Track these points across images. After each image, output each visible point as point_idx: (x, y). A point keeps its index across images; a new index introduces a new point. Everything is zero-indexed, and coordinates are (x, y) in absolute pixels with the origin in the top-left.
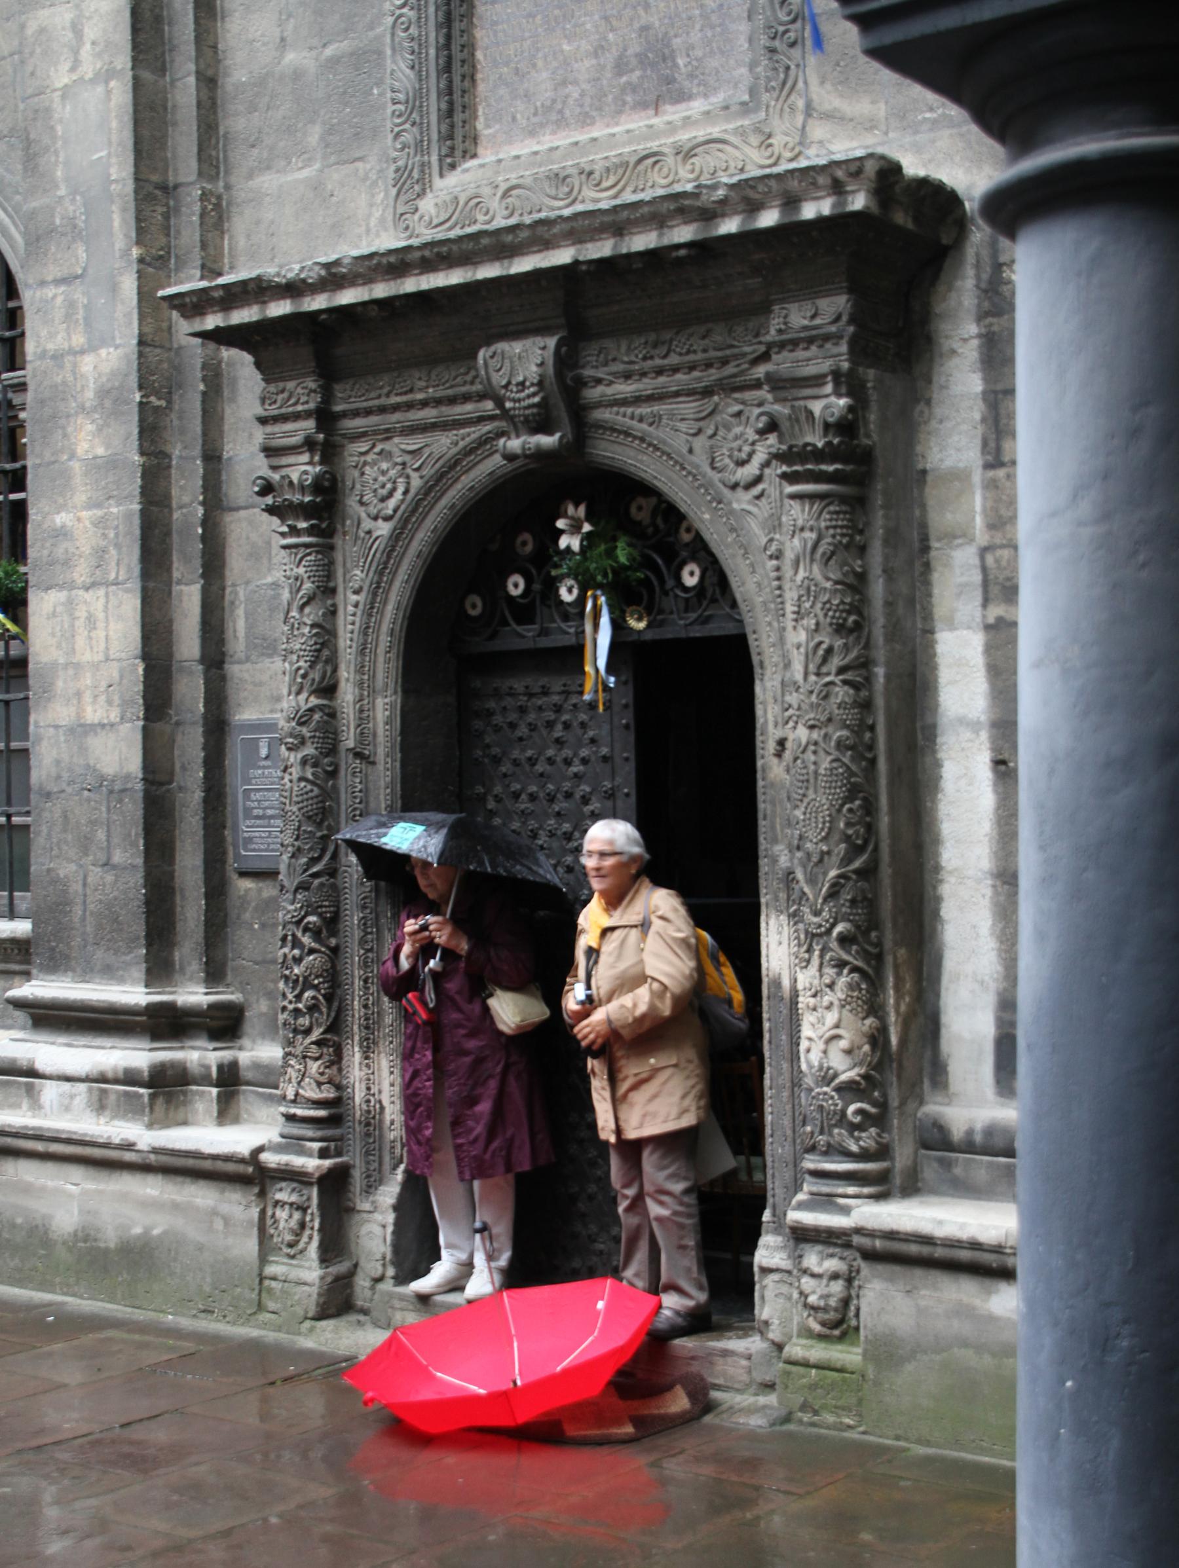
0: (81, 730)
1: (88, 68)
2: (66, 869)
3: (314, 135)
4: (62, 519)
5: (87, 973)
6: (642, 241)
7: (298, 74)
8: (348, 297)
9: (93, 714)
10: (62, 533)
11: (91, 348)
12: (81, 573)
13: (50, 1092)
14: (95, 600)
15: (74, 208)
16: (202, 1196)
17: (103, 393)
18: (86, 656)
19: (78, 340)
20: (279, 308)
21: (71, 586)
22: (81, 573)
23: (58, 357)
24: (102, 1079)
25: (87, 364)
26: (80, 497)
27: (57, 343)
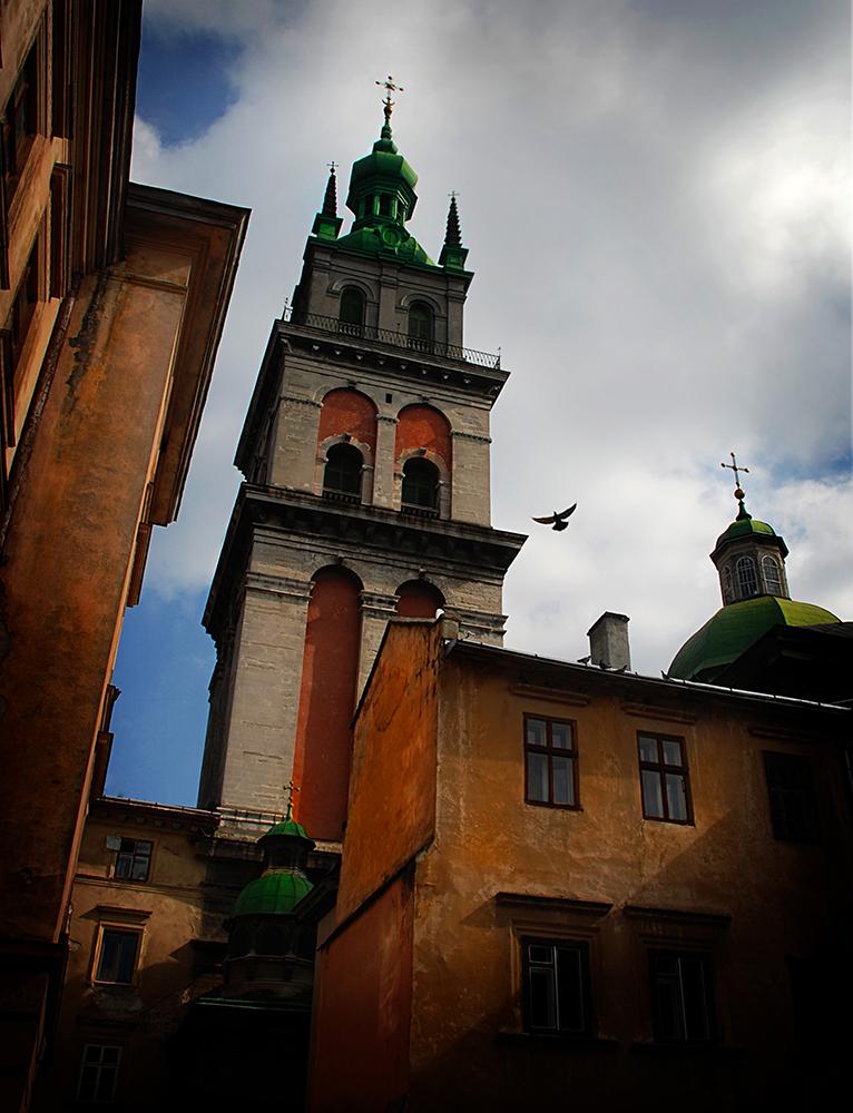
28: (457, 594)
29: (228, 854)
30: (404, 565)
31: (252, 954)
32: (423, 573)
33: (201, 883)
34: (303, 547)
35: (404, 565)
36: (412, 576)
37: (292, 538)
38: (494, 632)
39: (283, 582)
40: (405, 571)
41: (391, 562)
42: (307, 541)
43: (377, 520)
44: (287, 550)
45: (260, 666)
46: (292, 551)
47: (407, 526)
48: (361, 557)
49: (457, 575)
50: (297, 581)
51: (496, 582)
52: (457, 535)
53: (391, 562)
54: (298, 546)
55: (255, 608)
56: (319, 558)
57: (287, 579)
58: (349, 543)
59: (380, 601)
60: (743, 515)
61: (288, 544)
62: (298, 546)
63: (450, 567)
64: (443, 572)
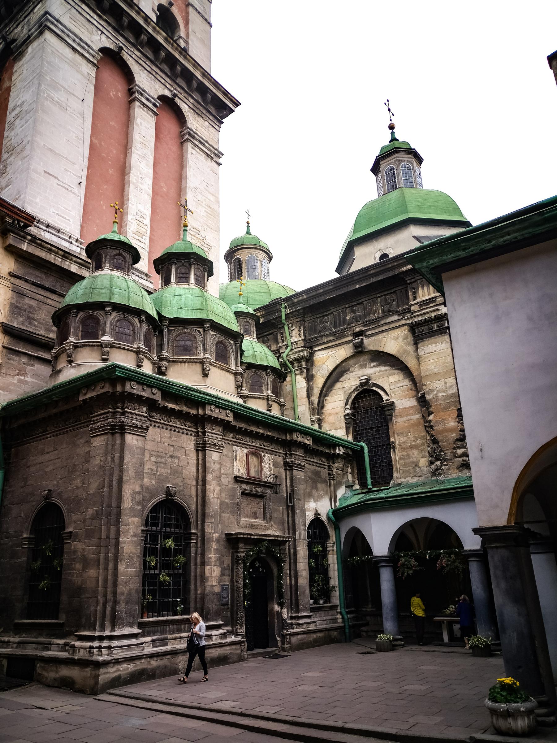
0: (212, 586)
1: (215, 496)
2: (210, 606)
3: (229, 511)
4: (210, 556)
5: (213, 620)
6: (279, 539)
7: (227, 503)
8: (256, 537)
9: (214, 584)
10: (210, 558)
11: (215, 533)
12: (213, 564)
13: (214, 638)
14: (215, 568)
15: (213, 513)
16: (234, 647)
17: (216, 539)
18: (213, 575)
19: (213, 531)
20: (249, 537)
21: (211, 565)
22: (213, 564)
23: (210, 533)
24: (221, 634)
25: (214, 535)
26: (213, 553)
27: (210, 531)
28: (194, 122)
29: (42, 254)
30: (163, 81)
31: (107, 338)
32: (175, 95)
33: (11, 274)
34: (92, 20)
35: (163, 81)
36: (168, 94)
37: (83, 6)
38: (216, 162)
39: (78, 40)
40: (163, 87)
41: (154, 73)
42: (95, 17)
43: (150, 30)
44: (79, 15)
45: (57, 102)
46: (82, 17)
47: (170, 49)
48: (134, 56)
49: (195, 109)
50: (89, 46)
51: (216, 127)
52: (200, 77)
53: (154, 73)
54: (88, 17)
55: (54, 50)
56: (103, 37)
57: (81, 39)
58: (126, 39)
59: (148, 99)
60: (394, 139)
61: (80, 10)
62: (88, 17)
63: (191, 100)
64: (186, 100)
